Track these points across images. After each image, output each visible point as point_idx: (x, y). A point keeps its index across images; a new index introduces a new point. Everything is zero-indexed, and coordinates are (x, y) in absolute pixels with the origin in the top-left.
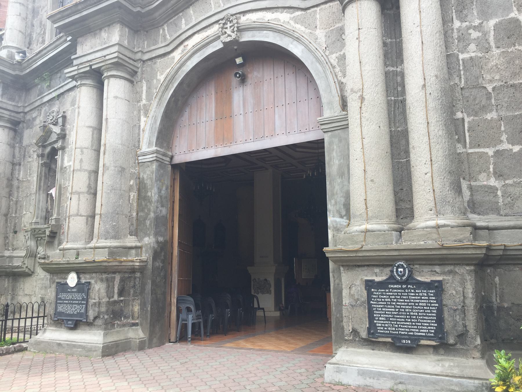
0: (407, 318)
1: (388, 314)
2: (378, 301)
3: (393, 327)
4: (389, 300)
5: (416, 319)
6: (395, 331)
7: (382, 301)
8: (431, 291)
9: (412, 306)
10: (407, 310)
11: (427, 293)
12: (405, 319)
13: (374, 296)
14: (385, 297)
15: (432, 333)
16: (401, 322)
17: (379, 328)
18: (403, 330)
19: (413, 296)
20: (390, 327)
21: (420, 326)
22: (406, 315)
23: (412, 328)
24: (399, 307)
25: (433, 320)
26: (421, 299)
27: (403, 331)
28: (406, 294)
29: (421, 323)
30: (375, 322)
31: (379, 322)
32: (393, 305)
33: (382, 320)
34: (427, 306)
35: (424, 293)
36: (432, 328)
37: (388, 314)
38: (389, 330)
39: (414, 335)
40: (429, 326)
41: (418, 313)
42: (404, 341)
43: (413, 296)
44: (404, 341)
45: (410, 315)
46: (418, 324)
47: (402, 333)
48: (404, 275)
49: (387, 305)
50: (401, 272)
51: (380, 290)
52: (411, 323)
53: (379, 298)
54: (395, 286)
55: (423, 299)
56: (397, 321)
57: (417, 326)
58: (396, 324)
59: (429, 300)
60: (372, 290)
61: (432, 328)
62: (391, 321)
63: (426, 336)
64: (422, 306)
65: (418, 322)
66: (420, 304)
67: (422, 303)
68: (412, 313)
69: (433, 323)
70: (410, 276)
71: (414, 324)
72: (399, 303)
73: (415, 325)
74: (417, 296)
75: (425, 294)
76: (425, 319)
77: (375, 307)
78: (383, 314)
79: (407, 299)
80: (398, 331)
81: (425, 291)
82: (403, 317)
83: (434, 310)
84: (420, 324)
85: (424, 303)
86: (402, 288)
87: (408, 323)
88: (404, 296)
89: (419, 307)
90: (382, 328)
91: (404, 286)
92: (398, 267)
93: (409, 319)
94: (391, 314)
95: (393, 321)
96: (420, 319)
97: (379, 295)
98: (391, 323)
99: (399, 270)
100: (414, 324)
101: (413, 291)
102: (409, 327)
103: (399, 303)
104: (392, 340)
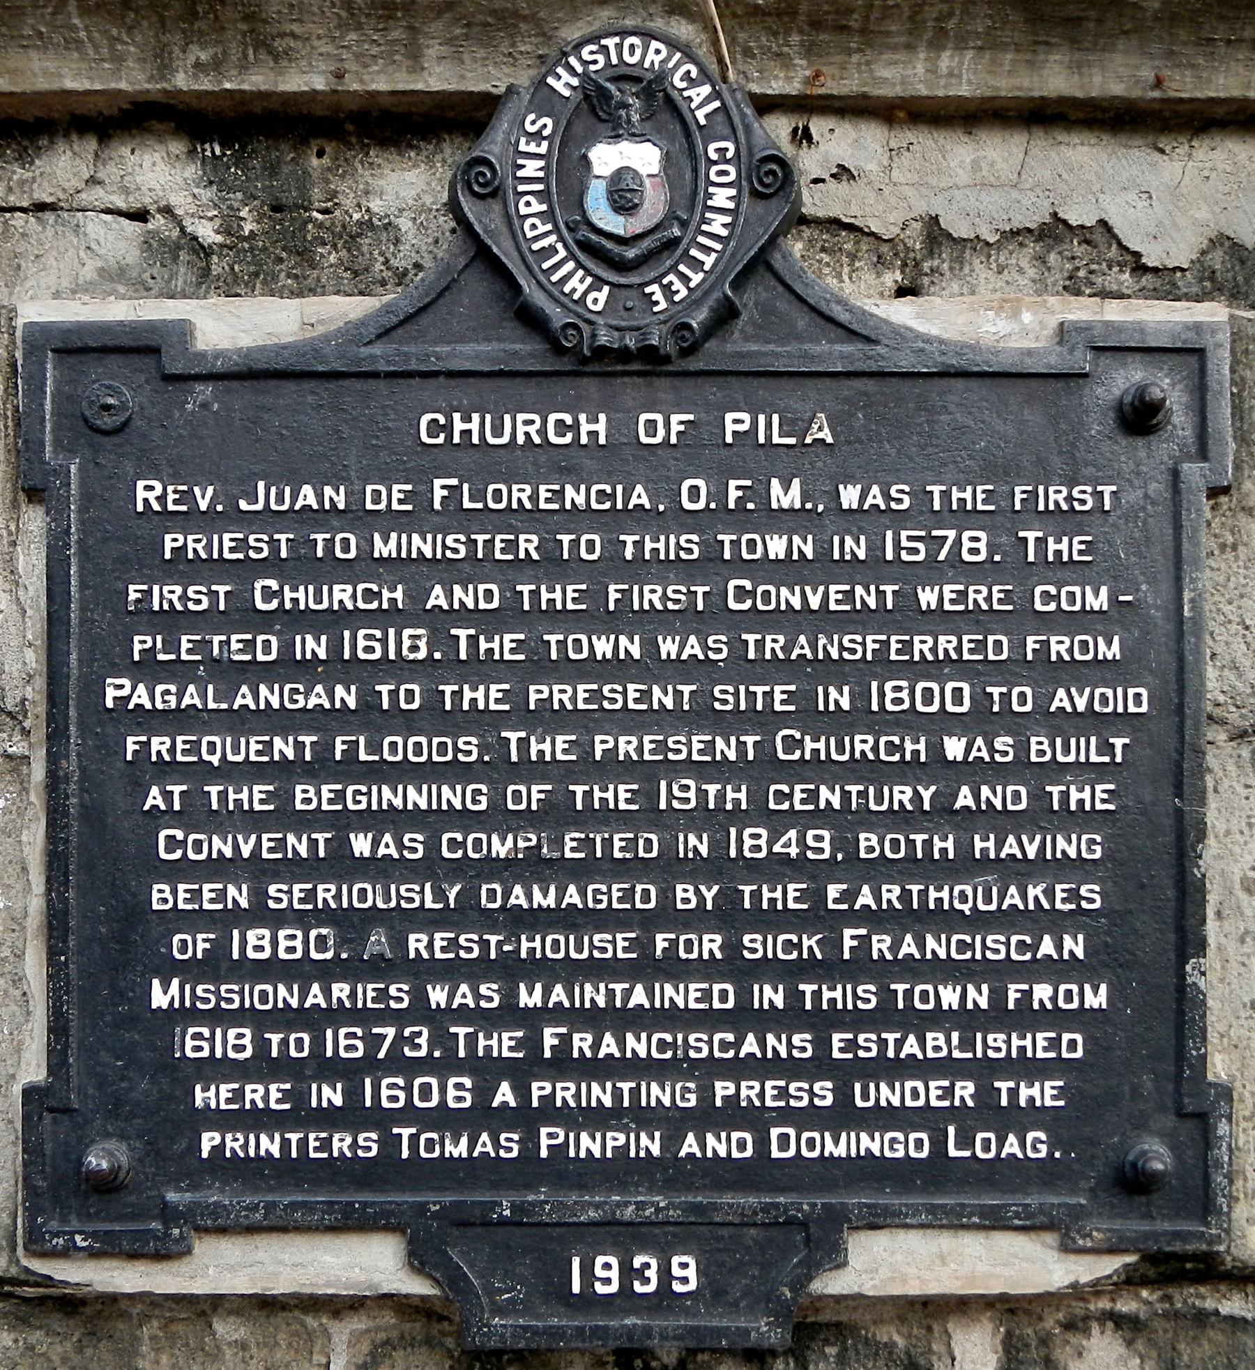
0: (667, 916)
1: (380, 870)
2: (230, 674)
3: (445, 1066)
4: (414, 642)
5: (816, 916)
6: (482, 1116)
7: (290, 668)
8: (1057, 496)
9: (766, 720)
10: (681, 794)
11: (1003, 520)
12: (648, 922)
13: (167, 595)
14: (342, 594)
15: (1018, 1119)
16: (572, 972)
17: (213, 1096)
18: (602, 1095)
19: (790, 570)
20: (398, 1064)
21: (857, 1020)
22: (670, 868)
23: (740, 1069)
24: (558, 747)
25: (1053, 922)
26: (908, 616)
27: (597, 1119)
28: (690, 544)
29: (883, 971)
30: (159, 999)
31: (233, 995)
32: (478, 720)
33: (273, 970)
34: (982, 720)
35: (964, 517)
36: (1038, 1044)
37: (380, 870)
38: (381, 1119)
39: (758, 1172)
40: (999, 1017)
41: (844, 822)
42: (607, 1273)
43: (790, 570)
44: (607, 1273)
45: (718, 867)
46: (833, 994)
47: (589, 1144)
48: (664, 248)
49: (370, 718)
50: (623, 194)
51: (264, 496)
52: (723, 994)
53: (242, 615)
54: (523, 426)
55: (938, 620)
56: (511, 970)
57: (823, 1022)
58: (488, 1020)
59: (1021, 618)
60: (147, 492)
61: (1038, 1044)
62: (424, 971)
63: (935, 1172)
64: (909, 721)
65: (829, 968)
66: (892, 694)
67: (916, 669)
68: (753, 841)
69: (1056, 970)
70: (758, 265)
71: (772, 996)
72: (561, 694)
73: (792, 1017)
74: (851, 570)
75: (975, 545)
76: (945, 920)
77: (167, 770)
78: (291, 869)
79: (686, 620)
80: (527, 1118)
81: (972, 496)
82: (609, 895)
83: (1087, 772)
84: (867, 996)
85: (936, 668)
86: (619, 457)
87: (687, 996)
88: (643, 569)
89: (862, 744)
90: (267, 1094)
91: (663, 425)
92: (598, 110)
93: (697, 920)
94: (430, 869)
95: (451, 972)
96: (876, 919)
97: (244, 571)
98: (420, 1011)
99: (606, 157)
100: (772, 996)
101: (785, 496)
102: (700, 1045)
103: (561, 694)
104: (418, 1260)
